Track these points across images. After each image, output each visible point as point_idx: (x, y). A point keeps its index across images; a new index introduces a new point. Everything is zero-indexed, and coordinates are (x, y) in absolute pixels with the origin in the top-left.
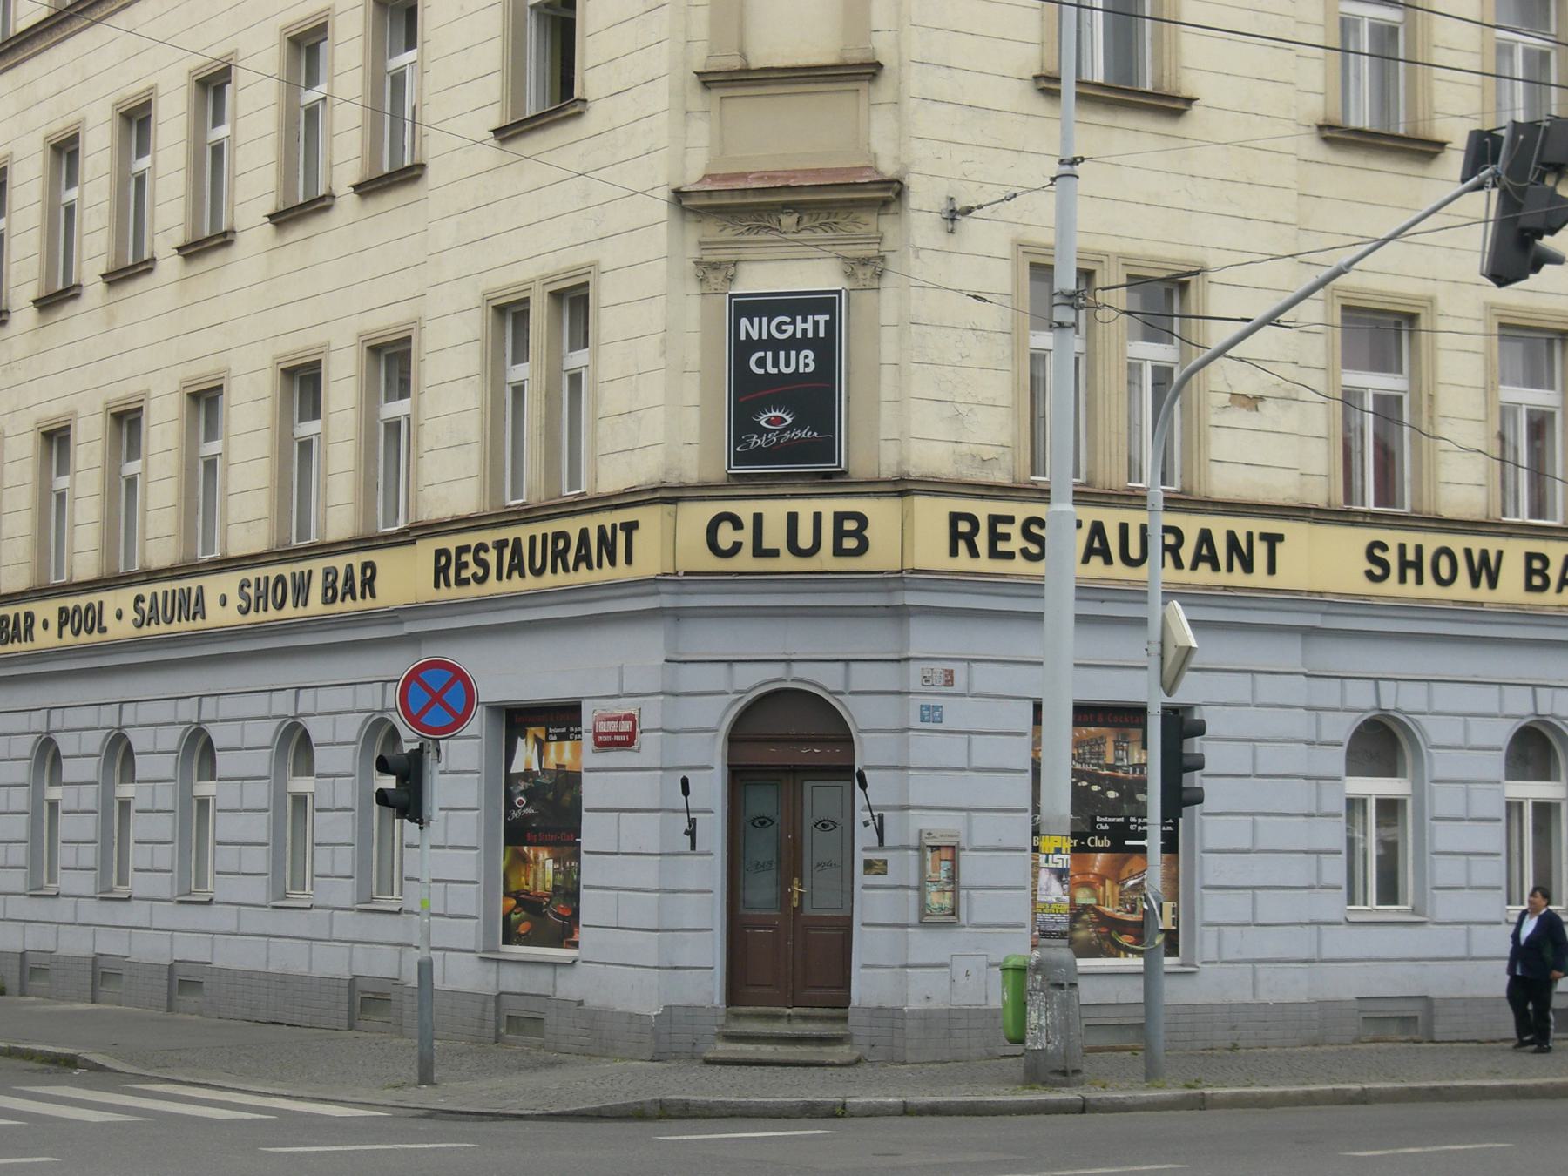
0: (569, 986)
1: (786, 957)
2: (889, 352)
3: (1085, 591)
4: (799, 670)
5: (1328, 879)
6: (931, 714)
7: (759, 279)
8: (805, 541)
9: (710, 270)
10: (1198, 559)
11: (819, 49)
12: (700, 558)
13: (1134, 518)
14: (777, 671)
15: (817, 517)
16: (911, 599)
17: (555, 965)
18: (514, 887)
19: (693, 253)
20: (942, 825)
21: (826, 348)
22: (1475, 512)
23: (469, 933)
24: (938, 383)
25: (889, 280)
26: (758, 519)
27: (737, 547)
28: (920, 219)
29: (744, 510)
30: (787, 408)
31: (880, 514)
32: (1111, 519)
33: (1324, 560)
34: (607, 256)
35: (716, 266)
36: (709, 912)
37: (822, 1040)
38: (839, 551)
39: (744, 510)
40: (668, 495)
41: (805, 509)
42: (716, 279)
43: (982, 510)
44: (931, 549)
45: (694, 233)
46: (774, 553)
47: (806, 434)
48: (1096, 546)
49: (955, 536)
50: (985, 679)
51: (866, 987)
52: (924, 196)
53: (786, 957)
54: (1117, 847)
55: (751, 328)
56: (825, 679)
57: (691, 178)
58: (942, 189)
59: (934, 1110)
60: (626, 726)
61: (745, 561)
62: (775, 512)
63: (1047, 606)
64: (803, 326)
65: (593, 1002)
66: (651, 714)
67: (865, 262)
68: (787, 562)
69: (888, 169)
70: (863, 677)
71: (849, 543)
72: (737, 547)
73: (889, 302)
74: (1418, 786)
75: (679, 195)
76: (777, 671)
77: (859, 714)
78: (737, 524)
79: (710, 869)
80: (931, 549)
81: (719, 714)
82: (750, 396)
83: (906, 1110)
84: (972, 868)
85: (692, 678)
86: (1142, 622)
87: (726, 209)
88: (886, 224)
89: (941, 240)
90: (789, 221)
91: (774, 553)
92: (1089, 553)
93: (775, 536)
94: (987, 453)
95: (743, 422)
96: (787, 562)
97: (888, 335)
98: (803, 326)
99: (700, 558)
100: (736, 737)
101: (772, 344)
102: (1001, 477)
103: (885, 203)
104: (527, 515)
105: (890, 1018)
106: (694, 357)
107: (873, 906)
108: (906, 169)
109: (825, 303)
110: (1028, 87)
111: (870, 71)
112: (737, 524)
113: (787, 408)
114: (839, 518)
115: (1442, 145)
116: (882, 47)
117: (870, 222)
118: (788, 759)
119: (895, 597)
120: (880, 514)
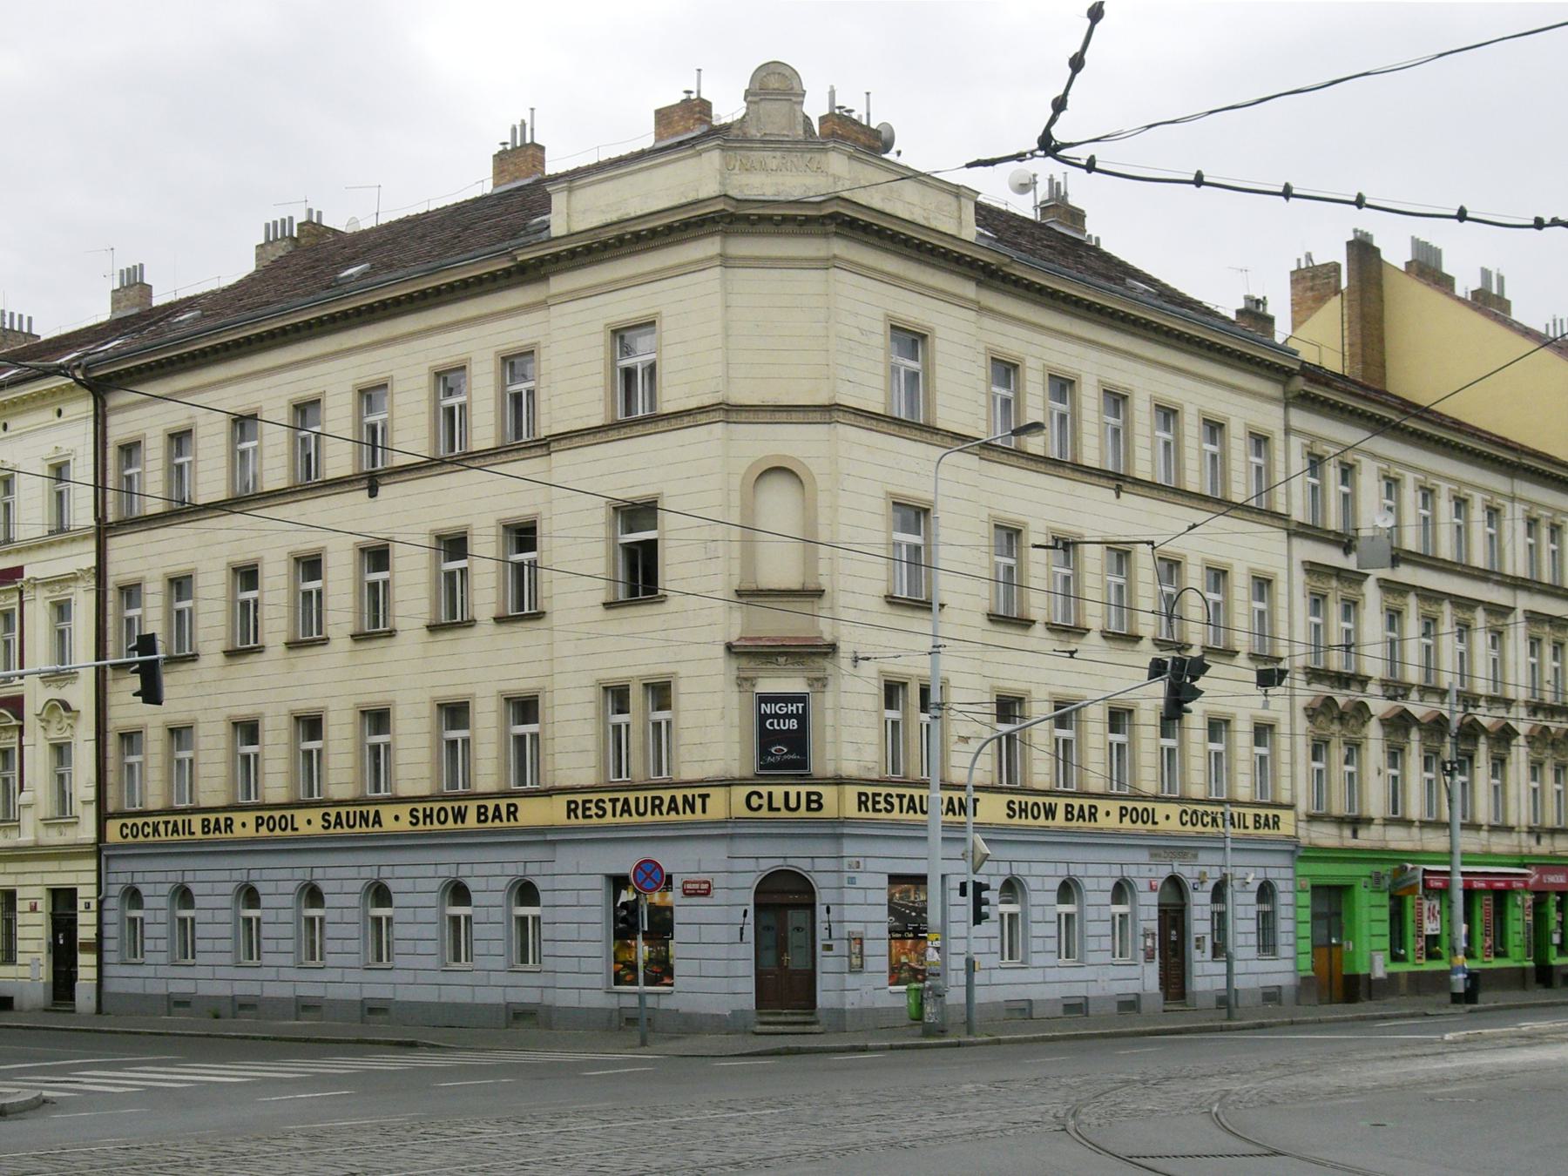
0: (666, 1003)
1: (786, 987)
2: (829, 721)
3: (947, 827)
4: (790, 862)
5: (1049, 948)
6: (852, 880)
7: (768, 685)
8: (793, 804)
9: (743, 681)
10: (909, 808)
11: (792, 581)
12: (741, 810)
13: (963, 795)
14: (780, 862)
15: (799, 794)
16: (846, 831)
17: (658, 994)
18: (621, 958)
19: (736, 673)
20: (857, 928)
21: (803, 719)
22: (1101, 790)
23: (598, 981)
24: (850, 736)
25: (830, 687)
26: (770, 794)
27: (760, 806)
28: (845, 662)
29: (764, 790)
30: (783, 744)
31: (828, 793)
32: (956, 795)
33: (993, 809)
34: (682, 670)
35: (746, 679)
36: (749, 968)
37: (806, 1023)
38: (809, 809)
39: (764, 790)
40: (727, 783)
41: (793, 790)
42: (747, 685)
43: (870, 790)
44: (851, 809)
45: (734, 663)
46: (778, 809)
47: (794, 757)
48: (950, 809)
49: (860, 802)
50: (872, 865)
51: (824, 999)
52: (845, 649)
53: (786, 987)
54: (916, 937)
55: (767, 709)
56: (803, 865)
57: (733, 638)
58: (851, 648)
59: (903, 1047)
60: (705, 886)
61: (764, 813)
62: (778, 792)
63: (940, 834)
64: (792, 708)
65: (684, 1009)
66: (719, 881)
67: (817, 679)
68: (784, 813)
69: (828, 638)
70: (821, 864)
71: (814, 806)
72: (760, 806)
73: (829, 698)
74: (1081, 907)
75: (729, 647)
76: (780, 862)
77: (818, 881)
78: (760, 796)
79: (749, 950)
80: (851, 809)
81: (752, 881)
82: (766, 739)
83: (892, 1048)
84: (868, 947)
85: (739, 865)
86: (964, 840)
87: (750, 654)
88: (827, 664)
89: (851, 669)
90: (782, 660)
91: (778, 809)
92: (948, 810)
93: (778, 801)
94: (870, 765)
95: (764, 750)
96: (784, 813)
97: (829, 713)
98: (792, 708)
99: (741, 810)
100: (758, 892)
101: (776, 716)
102: (875, 776)
103: (826, 654)
104: (1220, 803)
105: (840, 1013)
106: (736, 721)
107: (827, 965)
108: (837, 638)
109: (801, 698)
110: (882, 601)
111: (819, 593)
112: (760, 796)
113: (783, 744)
114: (809, 794)
115: (1141, 638)
116: (824, 583)
117: (820, 662)
118: (784, 902)
119: (837, 830)
120: (828, 793)
